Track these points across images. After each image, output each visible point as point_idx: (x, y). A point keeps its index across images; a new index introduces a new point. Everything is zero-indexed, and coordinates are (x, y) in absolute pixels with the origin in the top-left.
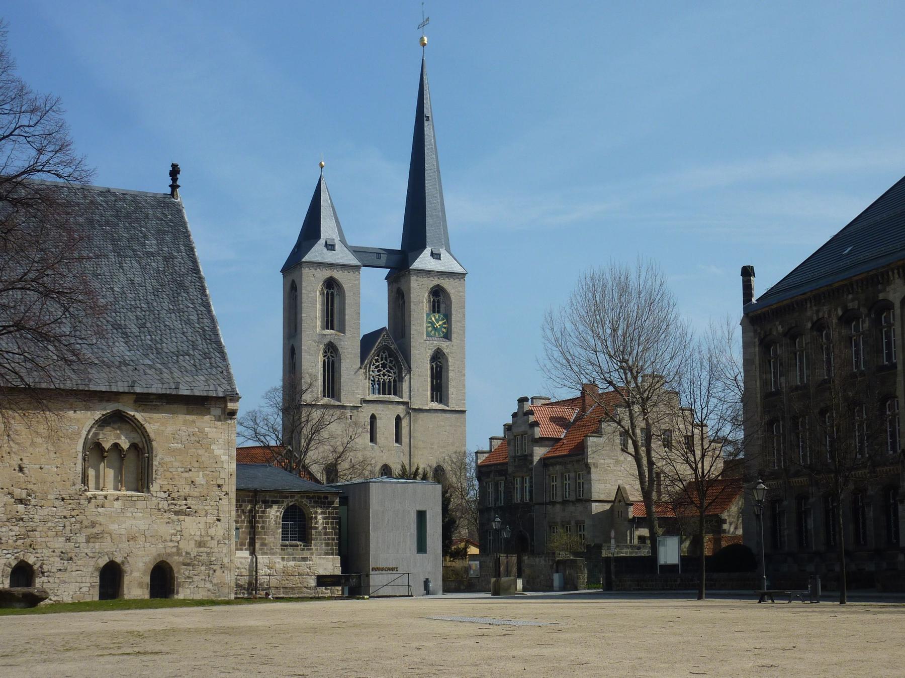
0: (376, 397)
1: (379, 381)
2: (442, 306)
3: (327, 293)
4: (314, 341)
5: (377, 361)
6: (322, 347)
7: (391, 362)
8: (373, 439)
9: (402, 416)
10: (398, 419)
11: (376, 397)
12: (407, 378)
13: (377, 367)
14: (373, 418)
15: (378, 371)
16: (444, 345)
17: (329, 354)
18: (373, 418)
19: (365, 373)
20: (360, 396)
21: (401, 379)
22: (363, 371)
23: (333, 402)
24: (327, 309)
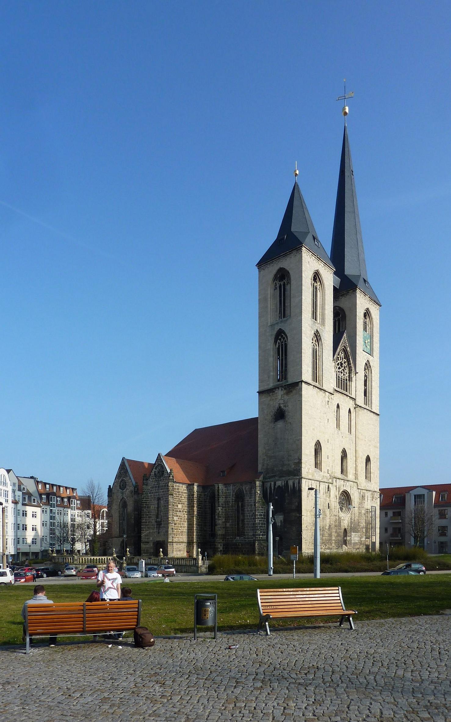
6: (313, 332)
7: (345, 362)
9: (352, 410)
10: (350, 411)
12: (354, 379)
14: (338, 406)
15: (339, 368)
16: (370, 358)
18: (338, 406)
21: (350, 379)
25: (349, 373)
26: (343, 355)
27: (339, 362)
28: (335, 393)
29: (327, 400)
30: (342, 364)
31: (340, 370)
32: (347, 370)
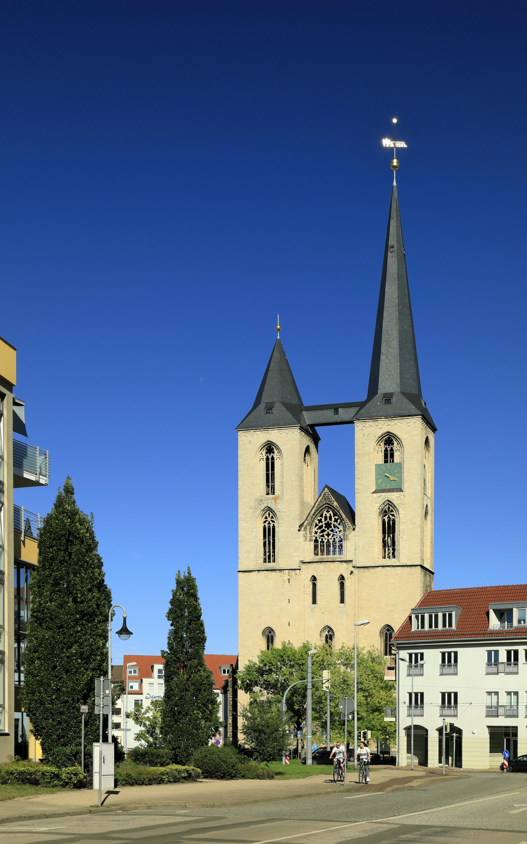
0: (319, 558)
1: (322, 542)
2: (396, 454)
3: (267, 459)
4: (251, 508)
5: (320, 521)
6: (259, 512)
7: (336, 520)
8: (314, 602)
10: (342, 578)
11: (319, 558)
13: (321, 527)
14: (314, 579)
15: (323, 531)
16: (393, 497)
17: (269, 519)
18: (314, 579)
19: (305, 536)
20: (298, 560)
22: (302, 532)
23: (271, 565)
24: (267, 475)
25: (344, 530)
26: (331, 512)
27: (321, 524)
28: (303, 567)
29: (287, 577)
30: (328, 525)
31: (326, 533)
32: (341, 528)
